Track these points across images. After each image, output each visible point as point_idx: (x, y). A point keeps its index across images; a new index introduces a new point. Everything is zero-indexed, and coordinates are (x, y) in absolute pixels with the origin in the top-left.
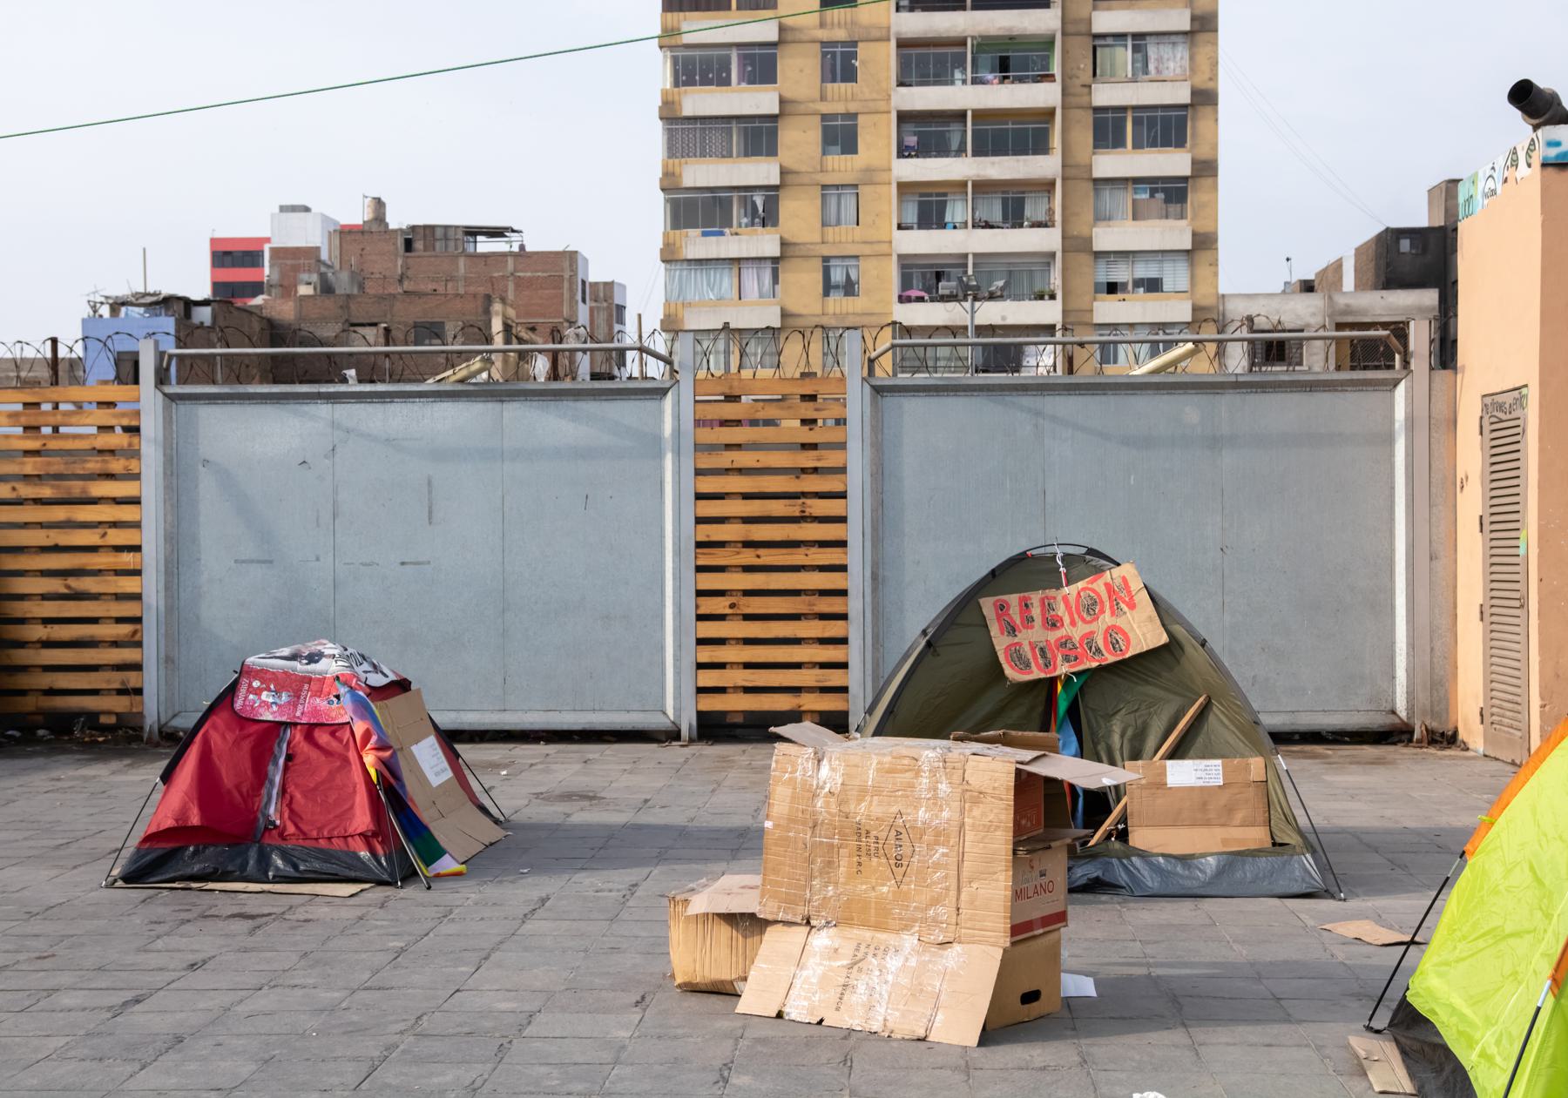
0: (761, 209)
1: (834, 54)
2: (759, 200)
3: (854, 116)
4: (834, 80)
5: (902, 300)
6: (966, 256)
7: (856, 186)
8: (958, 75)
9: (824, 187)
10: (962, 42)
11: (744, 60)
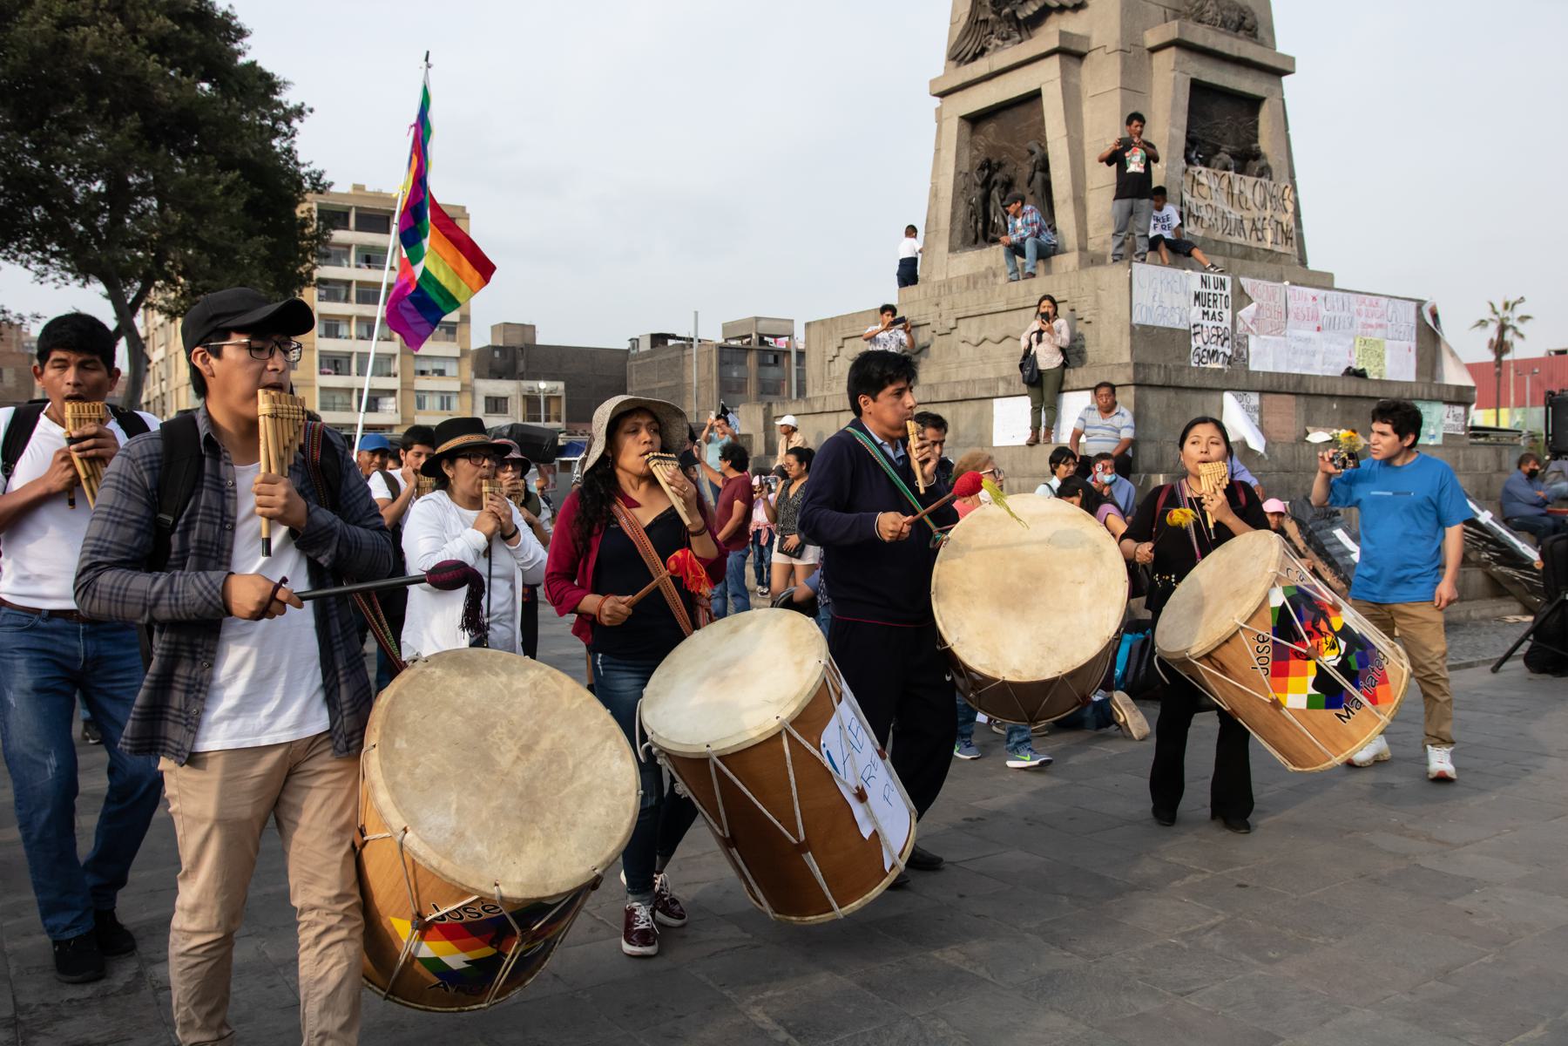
5: (322, 373)
6: (352, 353)
8: (345, 262)
10: (349, 246)
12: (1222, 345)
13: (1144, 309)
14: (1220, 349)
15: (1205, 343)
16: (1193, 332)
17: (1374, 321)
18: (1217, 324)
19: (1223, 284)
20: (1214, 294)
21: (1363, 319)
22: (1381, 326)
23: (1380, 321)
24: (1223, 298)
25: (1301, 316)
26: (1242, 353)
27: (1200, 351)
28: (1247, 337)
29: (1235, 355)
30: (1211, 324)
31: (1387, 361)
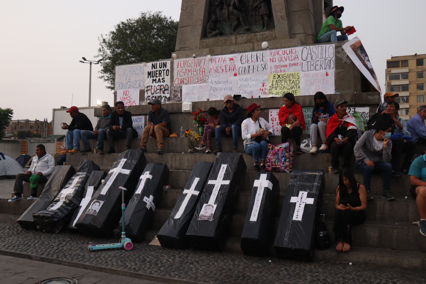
0: (405, 100)
1: (419, 74)
2: (405, 98)
3: (423, 84)
4: (419, 78)
7: (423, 96)
9: (417, 96)
11: (402, 75)
12: (164, 93)
13: (121, 84)
14: (162, 95)
15: (152, 94)
16: (146, 89)
17: (287, 63)
18: (162, 83)
19: (165, 65)
20: (159, 71)
21: (277, 63)
22: (295, 64)
23: (294, 62)
24: (165, 71)
25: (220, 70)
26: (177, 95)
27: (151, 98)
28: (182, 87)
29: (172, 97)
30: (156, 85)
31: (301, 85)
